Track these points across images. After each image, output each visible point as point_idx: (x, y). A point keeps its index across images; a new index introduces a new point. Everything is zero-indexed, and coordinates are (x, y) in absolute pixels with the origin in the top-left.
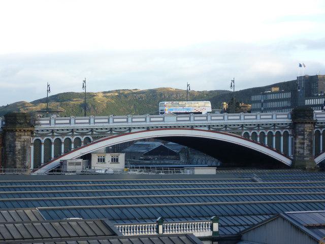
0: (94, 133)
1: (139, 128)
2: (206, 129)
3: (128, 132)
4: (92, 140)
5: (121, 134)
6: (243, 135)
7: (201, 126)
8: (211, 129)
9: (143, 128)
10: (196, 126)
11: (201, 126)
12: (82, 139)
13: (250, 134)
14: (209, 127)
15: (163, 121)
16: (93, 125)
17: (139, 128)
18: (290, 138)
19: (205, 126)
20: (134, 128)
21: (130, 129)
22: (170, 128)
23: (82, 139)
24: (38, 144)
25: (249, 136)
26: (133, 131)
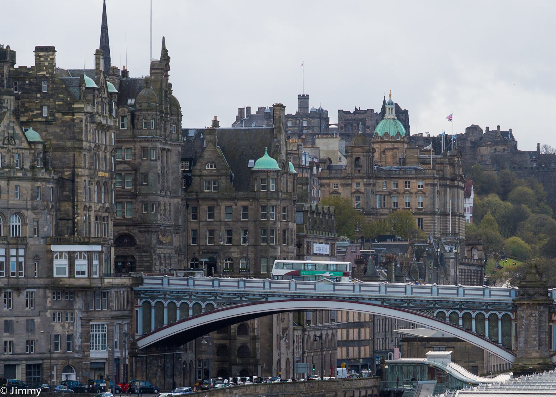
0: (218, 298)
1: (280, 296)
2: (379, 303)
3: (264, 300)
4: (216, 307)
5: (255, 302)
6: (435, 315)
7: (370, 299)
8: (385, 304)
9: (286, 296)
10: (363, 299)
11: (370, 299)
12: (203, 306)
13: (448, 314)
14: (383, 300)
15: (315, 289)
16: (269, 290)
17: (280, 296)
18: (513, 324)
19: (376, 299)
20: (273, 296)
21: (267, 296)
22: (324, 299)
23: (203, 306)
24: (147, 306)
25: (445, 317)
26: (270, 299)
